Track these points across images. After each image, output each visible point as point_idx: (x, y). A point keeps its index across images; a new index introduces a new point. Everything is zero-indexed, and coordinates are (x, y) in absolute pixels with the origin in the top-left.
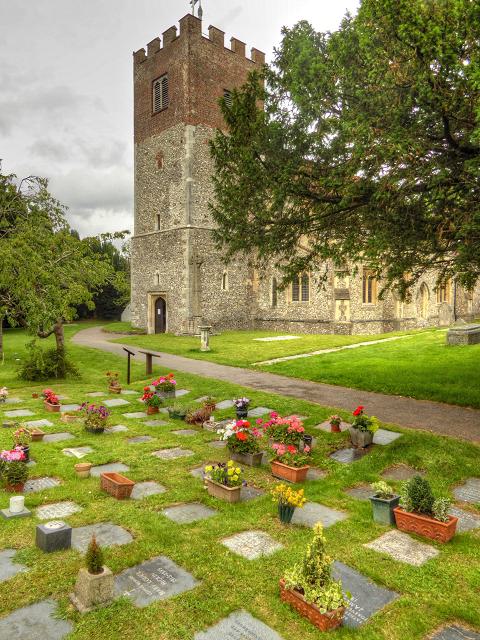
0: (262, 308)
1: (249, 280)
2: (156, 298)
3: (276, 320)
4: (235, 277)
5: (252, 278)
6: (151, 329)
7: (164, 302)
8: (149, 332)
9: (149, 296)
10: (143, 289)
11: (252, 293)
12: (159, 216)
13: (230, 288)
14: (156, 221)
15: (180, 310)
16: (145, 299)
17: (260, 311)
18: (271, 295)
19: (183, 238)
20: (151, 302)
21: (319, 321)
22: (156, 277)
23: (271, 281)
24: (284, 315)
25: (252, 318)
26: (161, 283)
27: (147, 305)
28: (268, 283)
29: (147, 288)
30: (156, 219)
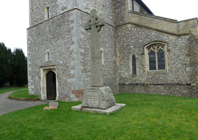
0: (124, 76)
1: (115, 57)
2: (46, 72)
3: (137, 84)
4: (107, 54)
5: (116, 56)
6: (43, 95)
7: (54, 74)
8: (42, 98)
9: (42, 70)
10: (36, 65)
11: (116, 66)
12: (48, 8)
13: (105, 62)
14: (46, 12)
15: (69, 80)
16: (38, 74)
17: (121, 78)
18: (131, 67)
19: (71, 18)
20: (43, 75)
21: (178, 84)
22: (47, 56)
23: (131, 57)
24: (143, 80)
25: (118, 83)
26: (51, 59)
27: (40, 77)
28: (128, 59)
29: (40, 64)
30: (46, 10)
